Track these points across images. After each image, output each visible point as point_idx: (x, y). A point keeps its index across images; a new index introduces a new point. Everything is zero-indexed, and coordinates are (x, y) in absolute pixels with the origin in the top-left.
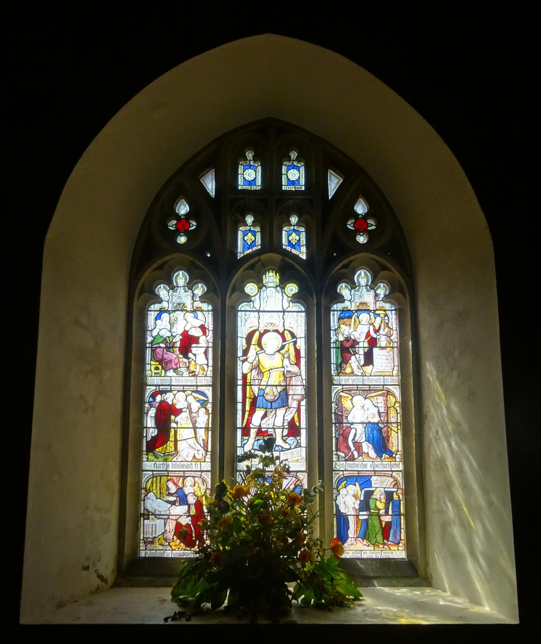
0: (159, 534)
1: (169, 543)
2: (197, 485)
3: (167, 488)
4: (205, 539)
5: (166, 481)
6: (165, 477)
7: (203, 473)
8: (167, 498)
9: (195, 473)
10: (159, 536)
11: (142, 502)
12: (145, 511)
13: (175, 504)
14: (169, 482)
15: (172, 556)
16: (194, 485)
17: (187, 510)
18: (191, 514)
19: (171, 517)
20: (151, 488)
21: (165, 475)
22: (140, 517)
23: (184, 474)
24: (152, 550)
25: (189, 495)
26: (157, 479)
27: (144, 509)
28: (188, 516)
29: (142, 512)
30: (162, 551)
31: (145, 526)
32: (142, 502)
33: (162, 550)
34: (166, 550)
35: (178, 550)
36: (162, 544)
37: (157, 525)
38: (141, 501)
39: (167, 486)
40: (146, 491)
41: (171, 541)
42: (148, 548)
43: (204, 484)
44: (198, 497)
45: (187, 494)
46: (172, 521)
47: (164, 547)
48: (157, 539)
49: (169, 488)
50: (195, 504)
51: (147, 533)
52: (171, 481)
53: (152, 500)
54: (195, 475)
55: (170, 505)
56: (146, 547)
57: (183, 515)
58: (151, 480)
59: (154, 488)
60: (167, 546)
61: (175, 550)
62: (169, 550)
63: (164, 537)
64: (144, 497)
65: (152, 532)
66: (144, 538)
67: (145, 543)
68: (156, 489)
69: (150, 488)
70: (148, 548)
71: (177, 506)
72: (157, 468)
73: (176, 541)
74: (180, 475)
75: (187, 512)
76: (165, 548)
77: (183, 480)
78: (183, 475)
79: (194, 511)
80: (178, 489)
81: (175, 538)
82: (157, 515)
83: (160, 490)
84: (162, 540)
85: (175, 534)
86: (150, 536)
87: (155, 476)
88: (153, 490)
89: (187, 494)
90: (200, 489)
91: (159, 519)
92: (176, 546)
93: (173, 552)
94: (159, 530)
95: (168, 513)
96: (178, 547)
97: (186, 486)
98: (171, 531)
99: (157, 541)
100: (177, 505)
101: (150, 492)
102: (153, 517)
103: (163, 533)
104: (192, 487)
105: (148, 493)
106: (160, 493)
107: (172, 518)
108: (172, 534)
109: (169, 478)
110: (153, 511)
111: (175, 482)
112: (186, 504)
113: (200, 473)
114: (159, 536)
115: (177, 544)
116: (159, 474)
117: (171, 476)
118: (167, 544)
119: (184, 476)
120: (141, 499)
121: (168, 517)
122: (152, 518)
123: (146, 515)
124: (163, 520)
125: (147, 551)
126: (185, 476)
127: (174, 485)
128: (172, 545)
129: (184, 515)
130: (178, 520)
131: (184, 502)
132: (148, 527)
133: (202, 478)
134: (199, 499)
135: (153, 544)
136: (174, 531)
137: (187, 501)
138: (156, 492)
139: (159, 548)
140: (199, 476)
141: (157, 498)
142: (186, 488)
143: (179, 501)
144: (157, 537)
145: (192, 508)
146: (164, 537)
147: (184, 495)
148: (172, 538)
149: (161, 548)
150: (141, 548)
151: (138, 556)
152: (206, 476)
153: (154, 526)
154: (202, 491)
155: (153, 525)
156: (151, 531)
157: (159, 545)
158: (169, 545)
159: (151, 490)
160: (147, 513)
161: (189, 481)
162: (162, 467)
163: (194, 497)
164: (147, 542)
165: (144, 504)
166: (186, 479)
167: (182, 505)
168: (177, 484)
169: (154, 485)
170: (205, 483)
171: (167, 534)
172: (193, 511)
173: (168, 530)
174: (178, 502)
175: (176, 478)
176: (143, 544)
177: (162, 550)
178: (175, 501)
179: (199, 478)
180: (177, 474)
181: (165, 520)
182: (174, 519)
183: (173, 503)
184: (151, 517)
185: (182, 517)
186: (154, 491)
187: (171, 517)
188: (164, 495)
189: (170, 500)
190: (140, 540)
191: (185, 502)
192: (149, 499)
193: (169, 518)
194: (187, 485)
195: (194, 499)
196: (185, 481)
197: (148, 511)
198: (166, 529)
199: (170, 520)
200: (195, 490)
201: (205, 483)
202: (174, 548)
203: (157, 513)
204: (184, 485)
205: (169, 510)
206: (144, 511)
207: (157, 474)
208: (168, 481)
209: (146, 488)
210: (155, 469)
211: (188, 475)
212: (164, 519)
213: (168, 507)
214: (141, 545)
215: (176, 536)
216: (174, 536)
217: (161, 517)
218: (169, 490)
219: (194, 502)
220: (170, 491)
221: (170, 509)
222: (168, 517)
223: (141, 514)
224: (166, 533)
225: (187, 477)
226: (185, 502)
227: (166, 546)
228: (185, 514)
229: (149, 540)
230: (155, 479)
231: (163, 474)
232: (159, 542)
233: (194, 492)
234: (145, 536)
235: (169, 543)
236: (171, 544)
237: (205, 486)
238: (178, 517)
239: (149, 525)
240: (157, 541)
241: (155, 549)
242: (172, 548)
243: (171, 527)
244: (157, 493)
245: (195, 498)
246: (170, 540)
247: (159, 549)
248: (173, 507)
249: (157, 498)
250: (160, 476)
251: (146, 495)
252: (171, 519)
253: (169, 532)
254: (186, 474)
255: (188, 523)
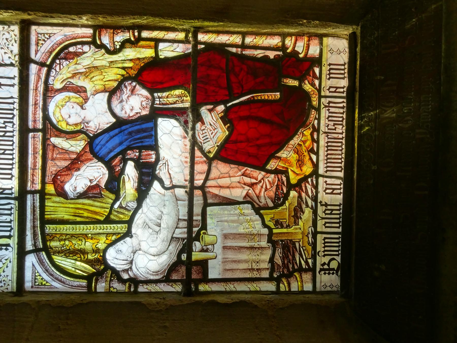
0: (260, 222)
1: (291, 187)
2: (79, 82)
3: (89, 198)
4: (280, 53)
5: (62, 199)
6: (48, 203)
7: (33, 56)
8: (128, 199)
9: (32, 86)
10: (267, 223)
11: (141, 289)
12: (175, 277)
13: (153, 166)
14: (68, 188)
15: (341, 174)
16: (80, 90)
17: (173, 122)
18: (187, 105)
19: (198, 182)
20: (90, 257)
21: (38, 204)
22: (198, 299)
23: (35, 130)
24: (314, 245)
25: (117, 110)
26: (53, 237)
27: (167, 279)
28: (198, 118)
29: (178, 288)
30: (320, 209)
31: (229, 275)
32: (141, 289)
33: (315, 212)
34: (315, 199)
35: (317, 154)
36: (295, 210)
37: (225, 232)
38: (136, 292)
39: (83, 195)
40: (99, 275)
41: (284, 179)
42: (307, 263)
43: (77, 55)
44: (125, 79)
45: (114, 120)
46: (212, 175)
47: (304, 206)
48: (275, 231)
49: (90, 188)
50: (152, 91)
51: (255, 267)
52: (64, 182)
53: (134, 252)
54: (41, 88)
55: (156, 184)
56: (306, 271)
57: (190, 133)
58: (58, 259)
59: (88, 245)
60: (303, 195)
61: (316, 166)
62: (316, 187)
63: (271, 204)
64: (123, 281)
65: (252, 248)
66: (270, 279)
67: (289, 275)
68: (94, 236)
69: (88, 262)
70: (307, 263)
71: (158, 159)
72: (9, 237)
73: (286, 160)
74: (40, 147)
75: (182, 119)
76: (310, 202)
77: (60, 133)
78: (40, 134)
79: (178, 92)
80: (92, 151)
81: (272, 165)
82: (190, 232)
83: (98, 222)
84: (280, 213)
85: (262, 167)
86: (266, 256)
87: (44, 241)
88: (96, 251)
89: (114, 120)
90: (96, 68)
91: (204, 226)
92: (300, 163)
93: (321, 171)
94: (246, 225)
95: (180, 192)
96: (306, 154)
97: (85, 122)
98: (247, 180)
99: (285, 230)
100: (153, 159)
101: (103, 261)
102: (197, 245)
103: (258, 210)
104: (86, 100)
105: (108, 267)
106: (108, 220)
107: (203, 176)
108: (260, 175)
109: (50, 189)
110: (174, 248)
111: (65, 164)
112: (150, 125)
113: (33, 68)
114: (264, 225)
115: (295, 156)
116: (34, 227)
117: (43, 183)
118: (293, 194)
119: (44, 131)
120: (129, 292)
121: (198, 193)
122: (202, 250)
123: (189, 273)
124: (209, 209)
125: (318, 267)
126: (44, 124)
127: (78, 169)
128: (299, 177)
129: (193, 129)
130: (211, 155)
131: (144, 130)
132: (235, 266)
133: (53, 61)
134: (133, 73)
135: (294, 244)
136: (249, 170)
137: (142, 119)
138: (103, 239)
139: (307, 221)
140: (45, 69)
141: (128, 234)
142: (91, 124)
143: (140, 149)
144: (270, 229)
145: (165, 100)
146: (271, 204)
147: (116, 131)
148: (273, 176)
149: (307, 214)
150: (308, 287)
151: (335, 298)
152: (46, 46)
153: (230, 243)
154: (104, 63)
155: (225, 248)
156: (248, 252)
157: (296, 223)
158: (298, 186)
159: (97, 256)
160: (183, 270)
161: (65, 112)
162: (8, 218)
163: (127, 91)
164: (285, 266)
165: (148, 282)
166: (55, 121)
167: (156, 140)
168: (74, 156)
169: (78, 244)
170: (71, 49)
171: (258, 197)
172: (179, 96)
173: (244, 193)
174: (145, 153)
175: (49, 163)
176: (292, 280)
177: (315, 212)
178: (139, 165)
179: (53, 73)
180: (35, 158)
181: (210, 201)
182: (205, 167)
183: (148, 174)
184: (196, 256)
185: (200, 138)
186: (101, 246)
187: (198, 182)
188: (116, 206)
189: (136, 185)
190: (278, 292)
191: (144, 126)
192: (131, 262)
193: (202, 188)
194: (79, 120)
195: (133, 91)
196: (63, 126)
197: (173, 268)
198: (241, 200)
199: (209, 183)
200: (99, 87)
201: (71, 49)
202: (308, 169)
203: (181, 233)
204: (80, 132)
205: (174, 187)
206: (175, 281)
207: (35, 235)
208: (62, 193)
209: (89, 278)
210: (14, 242)
211: (40, 114)
212: (206, 205)
213: (163, 191)
214: (295, 287)
215: (267, 162)
216: (268, 167)
217: (197, 218)
218: (97, 186)
219: (145, 92)
220: (103, 185)
221: (167, 183)
222: (198, 193)
223: (187, 292)
224: (255, 198)
225: (46, 118)
226: (144, 126)
227: (300, 197)
228: (190, 125)
229: (278, 260)
230: (53, 244)
231: (34, 211)
232: (286, 222)
233: (104, 91)
234: (266, 274)
235: (291, 187)
236: (294, 179)
237: (86, 48)
238: (198, 153)
239: (225, 261)
240: (285, 230)
241: (310, 236)
242: (311, 175)
243: (233, 179)
244: (107, 234)
245: (129, 88)
246: (280, 181)
247: (310, 223)
248: (161, 172)
249: (128, 234)
250: (44, 222)
251: (116, 273)
252: (206, 179)
253: (252, 185)
254: (35, 121)
255: (221, 118)
